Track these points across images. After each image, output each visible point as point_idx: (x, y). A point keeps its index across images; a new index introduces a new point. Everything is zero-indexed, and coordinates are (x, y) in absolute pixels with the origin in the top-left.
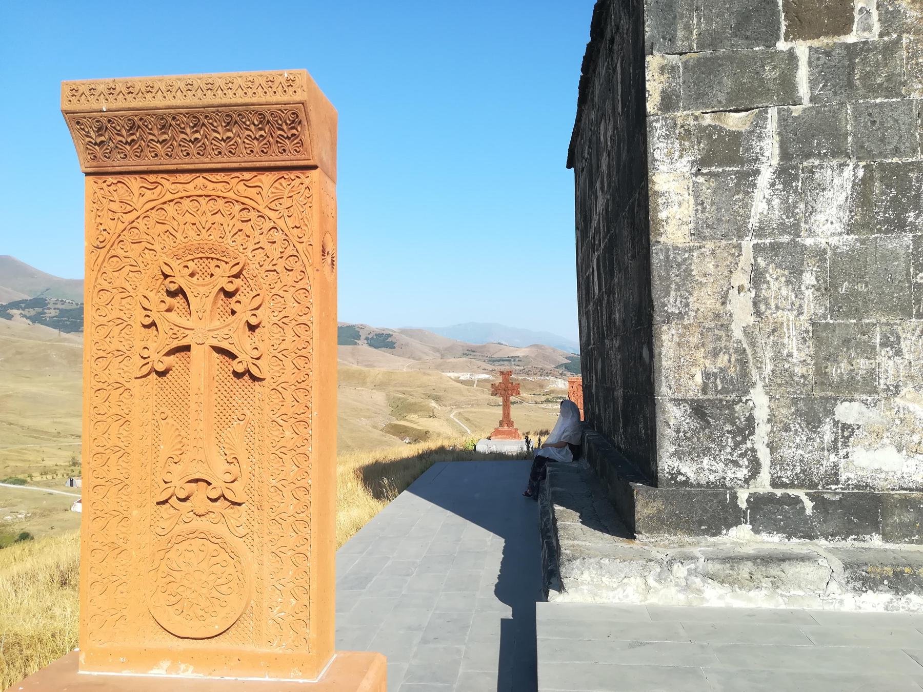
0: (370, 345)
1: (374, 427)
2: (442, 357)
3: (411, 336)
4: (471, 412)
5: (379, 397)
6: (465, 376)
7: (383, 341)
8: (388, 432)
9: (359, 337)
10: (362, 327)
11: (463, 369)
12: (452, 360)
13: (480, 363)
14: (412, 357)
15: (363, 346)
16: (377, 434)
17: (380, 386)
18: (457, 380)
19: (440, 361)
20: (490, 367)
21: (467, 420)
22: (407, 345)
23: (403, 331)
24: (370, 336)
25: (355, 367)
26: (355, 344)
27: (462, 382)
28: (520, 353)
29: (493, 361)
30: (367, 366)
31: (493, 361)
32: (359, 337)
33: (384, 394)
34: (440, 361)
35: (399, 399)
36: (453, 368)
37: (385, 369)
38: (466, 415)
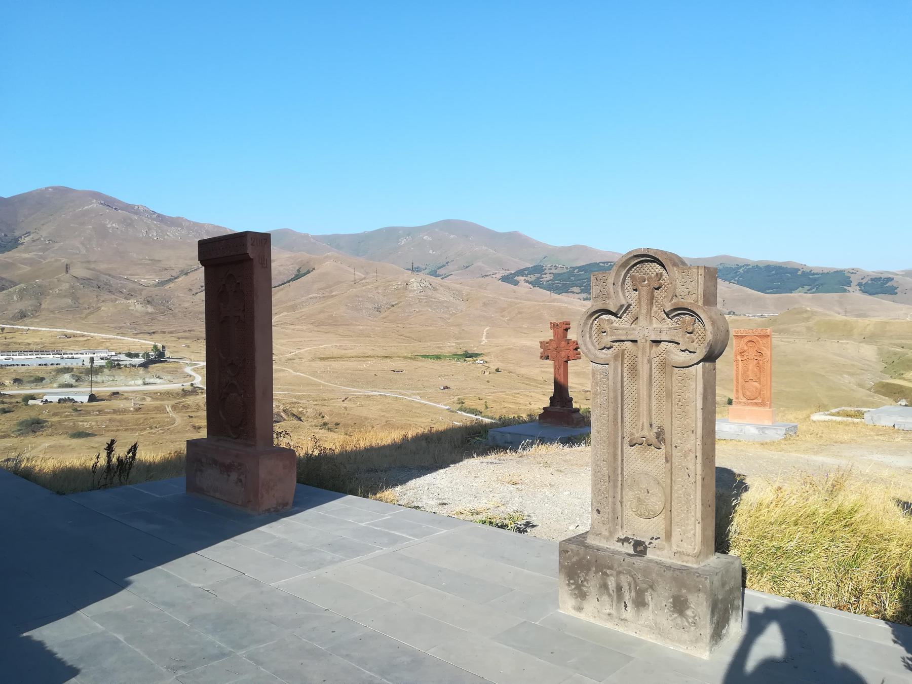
0: (864, 292)
1: (860, 385)
5: (869, 352)
7: (880, 286)
9: (849, 283)
10: (854, 272)
15: (854, 294)
16: (862, 393)
17: (870, 338)
24: (864, 282)
25: (841, 318)
26: (845, 291)
30: (859, 316)
32: (849, 283)
33: (875, 347)
35: (895, 354)
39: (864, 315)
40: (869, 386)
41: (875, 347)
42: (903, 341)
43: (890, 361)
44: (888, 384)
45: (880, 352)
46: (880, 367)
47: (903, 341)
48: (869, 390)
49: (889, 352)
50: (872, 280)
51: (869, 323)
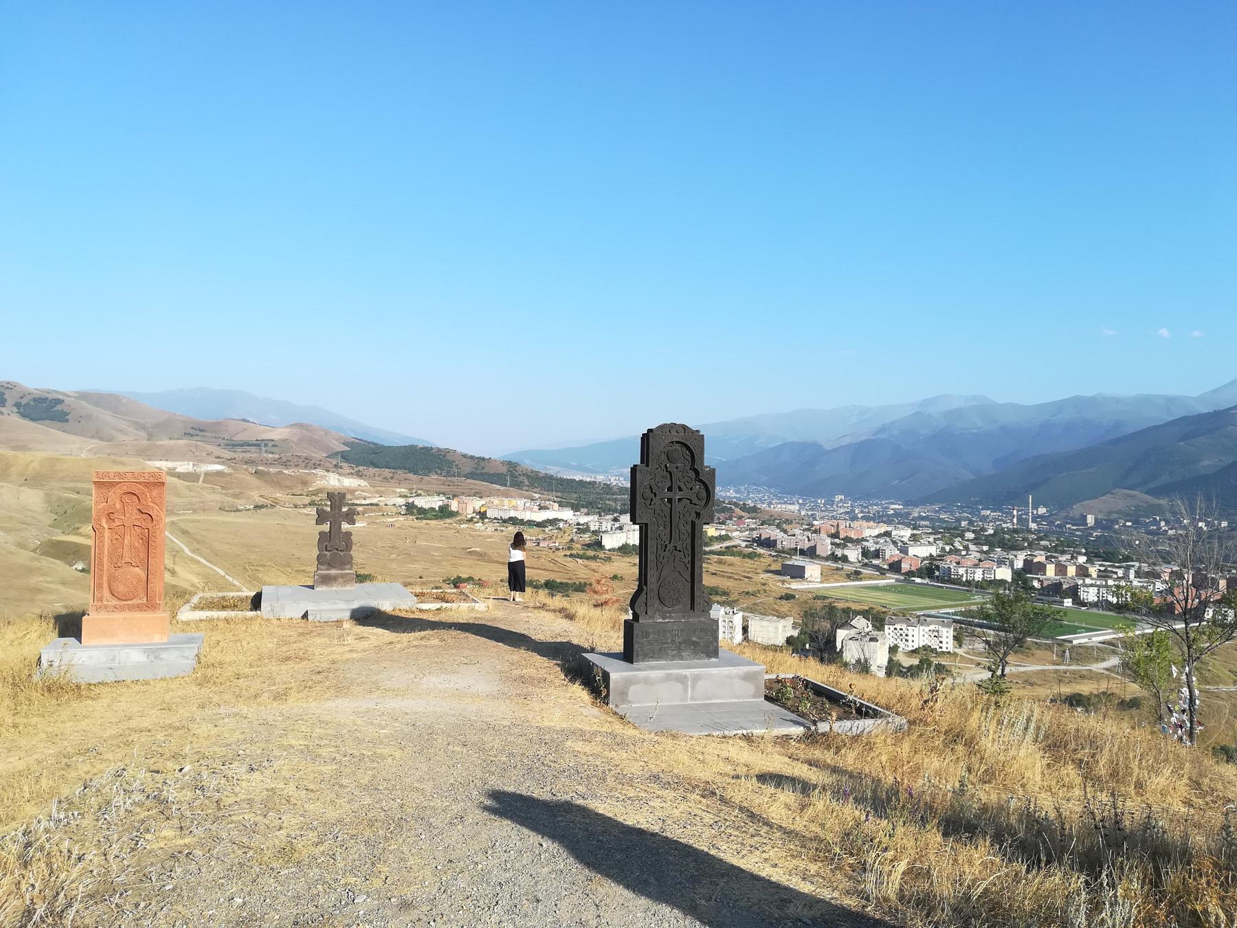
0: (23, 416)
1: (20, 545)
2: (150, 436)
3: (97, 404)
4: (192, 521)
5: (33, 499)
6: (184, 467)
7: (46, 409)
8: (45, 554)
10: (10, 386)
11: (182, 456)
12: (166, 442)
13: (210, 448)
14: (98, 435)
16: (24, 557)
17: (34, 480)
18: (172, 472)
19: (145, 443)
20: (227, 454)
21: (185, 532)
22: (89, 417)
23: (83, 396)
24: (24, 401)
27: (179, 476)
28: (275, 435)
29: (232, 445)
30: (16, 448)
31: (232, 445)
33: (41, 493)
34: (145, 443)
35: (68, 501)
36: (167, 455)
37: (45, 454)
38: (182, 525)
39: (24, 448)
40: (33, 546)
41: (41, 493)
42: (79, 485)
43: (61, 511)
44: (59, 542)
45: (48, 499)
46: (48, 519)
47: (79, 485)
48: (34, 551)
49: (59, 499)
50: (34, 400)
51: (33, 459)
